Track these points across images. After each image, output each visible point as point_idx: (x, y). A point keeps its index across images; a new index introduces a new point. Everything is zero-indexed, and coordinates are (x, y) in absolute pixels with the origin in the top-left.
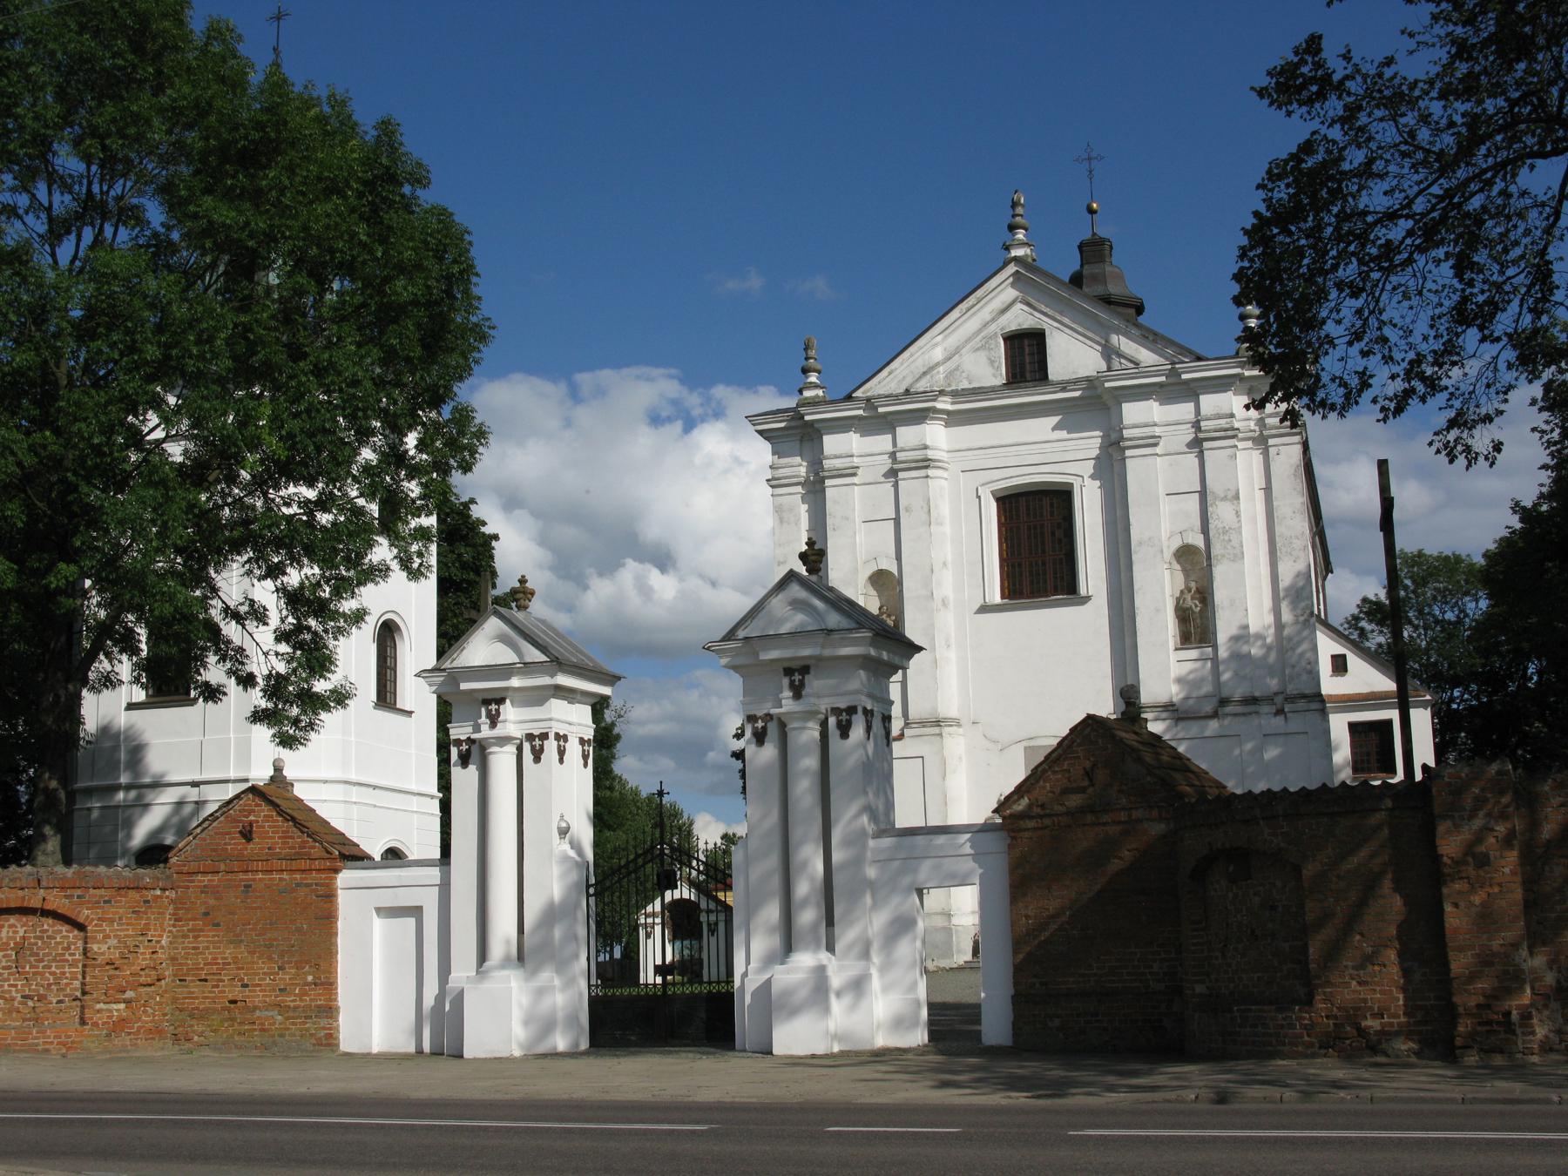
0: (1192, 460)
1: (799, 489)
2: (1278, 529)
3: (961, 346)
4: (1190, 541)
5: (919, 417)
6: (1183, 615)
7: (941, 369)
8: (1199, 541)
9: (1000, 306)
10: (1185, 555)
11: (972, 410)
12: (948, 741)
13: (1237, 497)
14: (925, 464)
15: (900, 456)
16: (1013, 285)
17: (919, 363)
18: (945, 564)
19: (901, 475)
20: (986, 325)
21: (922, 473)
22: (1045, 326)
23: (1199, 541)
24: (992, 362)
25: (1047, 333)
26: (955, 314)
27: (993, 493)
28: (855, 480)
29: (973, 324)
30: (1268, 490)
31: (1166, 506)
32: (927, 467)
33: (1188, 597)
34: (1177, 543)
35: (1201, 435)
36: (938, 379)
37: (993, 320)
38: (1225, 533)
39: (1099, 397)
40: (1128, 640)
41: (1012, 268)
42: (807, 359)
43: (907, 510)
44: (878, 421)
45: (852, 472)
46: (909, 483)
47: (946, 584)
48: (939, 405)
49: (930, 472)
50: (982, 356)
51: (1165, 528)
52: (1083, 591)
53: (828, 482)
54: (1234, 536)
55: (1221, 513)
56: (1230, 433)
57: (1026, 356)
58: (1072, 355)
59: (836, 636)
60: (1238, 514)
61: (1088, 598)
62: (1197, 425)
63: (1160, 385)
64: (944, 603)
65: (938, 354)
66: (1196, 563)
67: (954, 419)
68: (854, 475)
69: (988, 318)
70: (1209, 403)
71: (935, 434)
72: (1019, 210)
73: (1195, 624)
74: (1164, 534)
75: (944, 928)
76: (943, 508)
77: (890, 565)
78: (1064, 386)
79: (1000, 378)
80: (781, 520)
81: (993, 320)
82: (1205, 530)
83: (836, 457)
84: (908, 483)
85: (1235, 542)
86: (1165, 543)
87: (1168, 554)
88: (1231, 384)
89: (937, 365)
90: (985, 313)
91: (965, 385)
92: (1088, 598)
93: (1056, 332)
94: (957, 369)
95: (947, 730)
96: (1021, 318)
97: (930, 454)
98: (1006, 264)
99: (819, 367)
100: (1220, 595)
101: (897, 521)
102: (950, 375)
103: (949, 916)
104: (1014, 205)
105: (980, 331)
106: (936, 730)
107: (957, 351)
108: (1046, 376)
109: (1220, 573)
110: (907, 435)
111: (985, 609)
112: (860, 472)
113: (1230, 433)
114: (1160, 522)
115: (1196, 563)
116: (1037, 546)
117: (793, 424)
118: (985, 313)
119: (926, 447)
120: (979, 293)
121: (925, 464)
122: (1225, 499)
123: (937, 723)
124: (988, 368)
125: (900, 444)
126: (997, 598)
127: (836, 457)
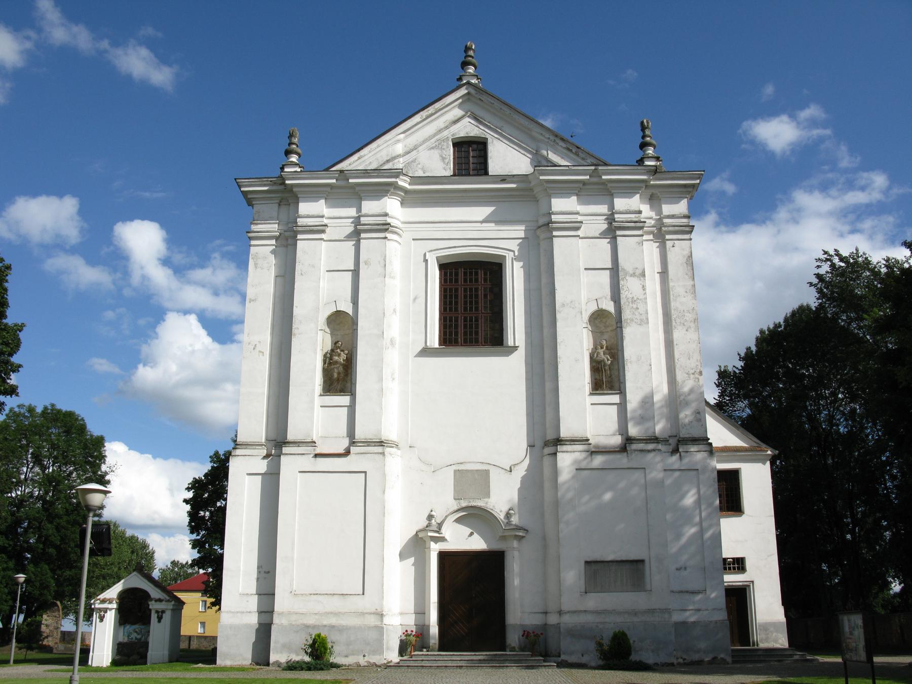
0: (605, 244)
2: (673, 305)
3: (420, 143)
4: (604, 307)
5: (381, 191)
6: (597, 367)
7: (401, 160)
8: (610, 307)
9: (450, 120)
10: (598, 318)
11: (425, 194)
12: (388, 459)
13: (644, 276)
14: (385, 228)
15: (363, 220)
16: (460, 106)
17: (384, 153)
18: (395, 311)
19: (363, 235)
20: (440, 131)
22: (488, 136)
23: (610, 307)
24: (443, 159)
25: (490, 141)
26: (417, 118)
27: (437, 258)
28: (323, 236)
29: (429, 129)
30: (664, 272)
31: (586, 278)
32: (386, 230)
33: (601, 351)
34: (593, 308)
35: (615, 224)
36: (399, 164)
37: (447, 128)
38: (633, 301)
39: (531, 190)
40: (549, 385)
41: (463, 91)
42: (290, 144)
43: (366, 263)
44: (350, 192)
45: (320, 230)
47: (394, 328)
48: (401, 183)
49: (389, 235)
50: (436, 154)
51: (584, 295)
53: (299, 237)
54: (641, 306)
55: (630, 287)
56: (638, 225)
57: (471, 156)
58: (507, 158)
59: (485, 98)
60: (644, 288)
61: (515, 348)
62: (610, 219)
63: (584, 183)
64: (392, 342)
65: (399, 148)
66: (608, 327)
67: (410, 199)
69: (442, 126)
70: (620, 203)
71: (392, 205)
72: (471, 53)
73: (607, 375)
74: (584, 301)
75: (376, 627)
76: (396, 264)
77: (348, 308)
78: (503, 179)
79: (450, 172)
81: (447, 128)
82: (616, 296)
84: (368, 244)
85: (642, 310)
86: (584, 307)
87: (586, 316)
88: (640, 188)
89: (399, 156)
90: (441, 122)
91: (420, 173)
93: (495, 141)
94: (414, 161)
95: (388, 450)
96: (468, 128)
97: (389, 220)
98: (459, 88)
99: (299, 151)
100: (629, 352)
101: (356, 273)
102: (408, 164)
103: (382, 615)
104: (467, 49)
105: (435, 135)
106: (380, 449)
107: (416, 148)
108: (486, 173)
109: (629, 333)
111: (426, 352)
112: (328, 230)
113: (638, 225)
114: (580, 286)
115: (608, 327)
116: (471, 305)
117: (275, 188)
118: (441, 122)
119: (386, 215)
120: (438, 105)
121: (385, 228)
122: (633, 275)
123: (381, 443)
124: (439, 163)
125: (364, 211)
126: (434, 341)
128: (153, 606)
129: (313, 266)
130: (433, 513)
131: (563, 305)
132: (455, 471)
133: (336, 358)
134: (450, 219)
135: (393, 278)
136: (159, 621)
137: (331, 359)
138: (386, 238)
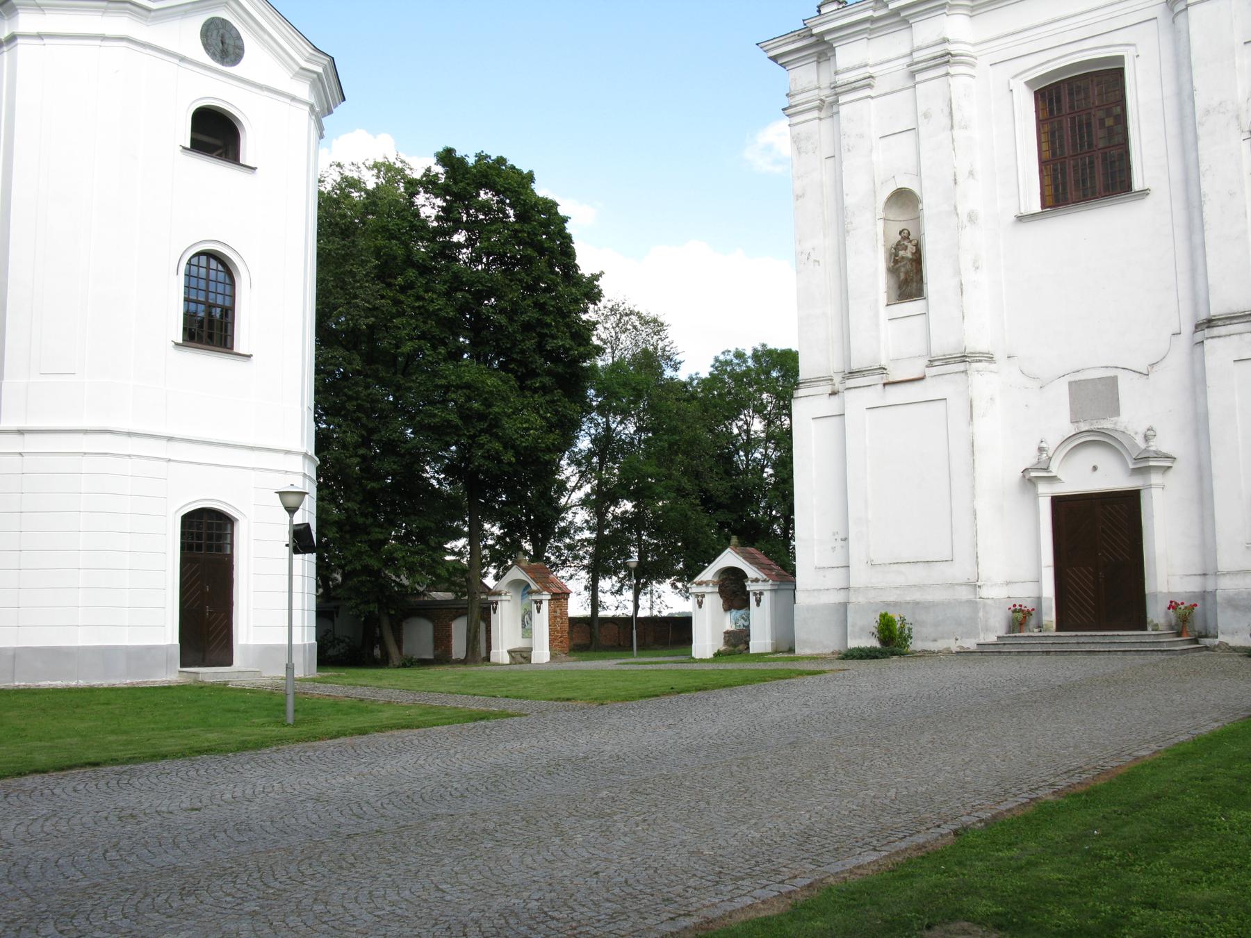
1: (815, 114)
14: (946, 59)
18: (971, 173)
21: (942, 71)
43: (926, 116)
45: (867, 82)
46: (930, 88)
49: (952, 70)
52: (1137, 185)
61: (1145, 193)
64: (972, 218)
68: (869, 86)
75: (969, 602)
80: (799, 149)
83: (848, 70)
92: (1145, 193)
95: (975, 365)
103: (975, 586)
106: (961, 367)
110: (927, 31)
111: (1021, 218)
112: (876, 83)
119: (945, 41)
121: (946, 59)
127: (848, 70)
128: (750, 587)
129: (862, 136)
130: (1043, 445)
131: (1208, 112)
132: (1070, 383)
133: (901, 253)
134: (1036, 22)
135: (965, 127)
136: (758, 605)
137: (896, 255)
138: (947, 74)
